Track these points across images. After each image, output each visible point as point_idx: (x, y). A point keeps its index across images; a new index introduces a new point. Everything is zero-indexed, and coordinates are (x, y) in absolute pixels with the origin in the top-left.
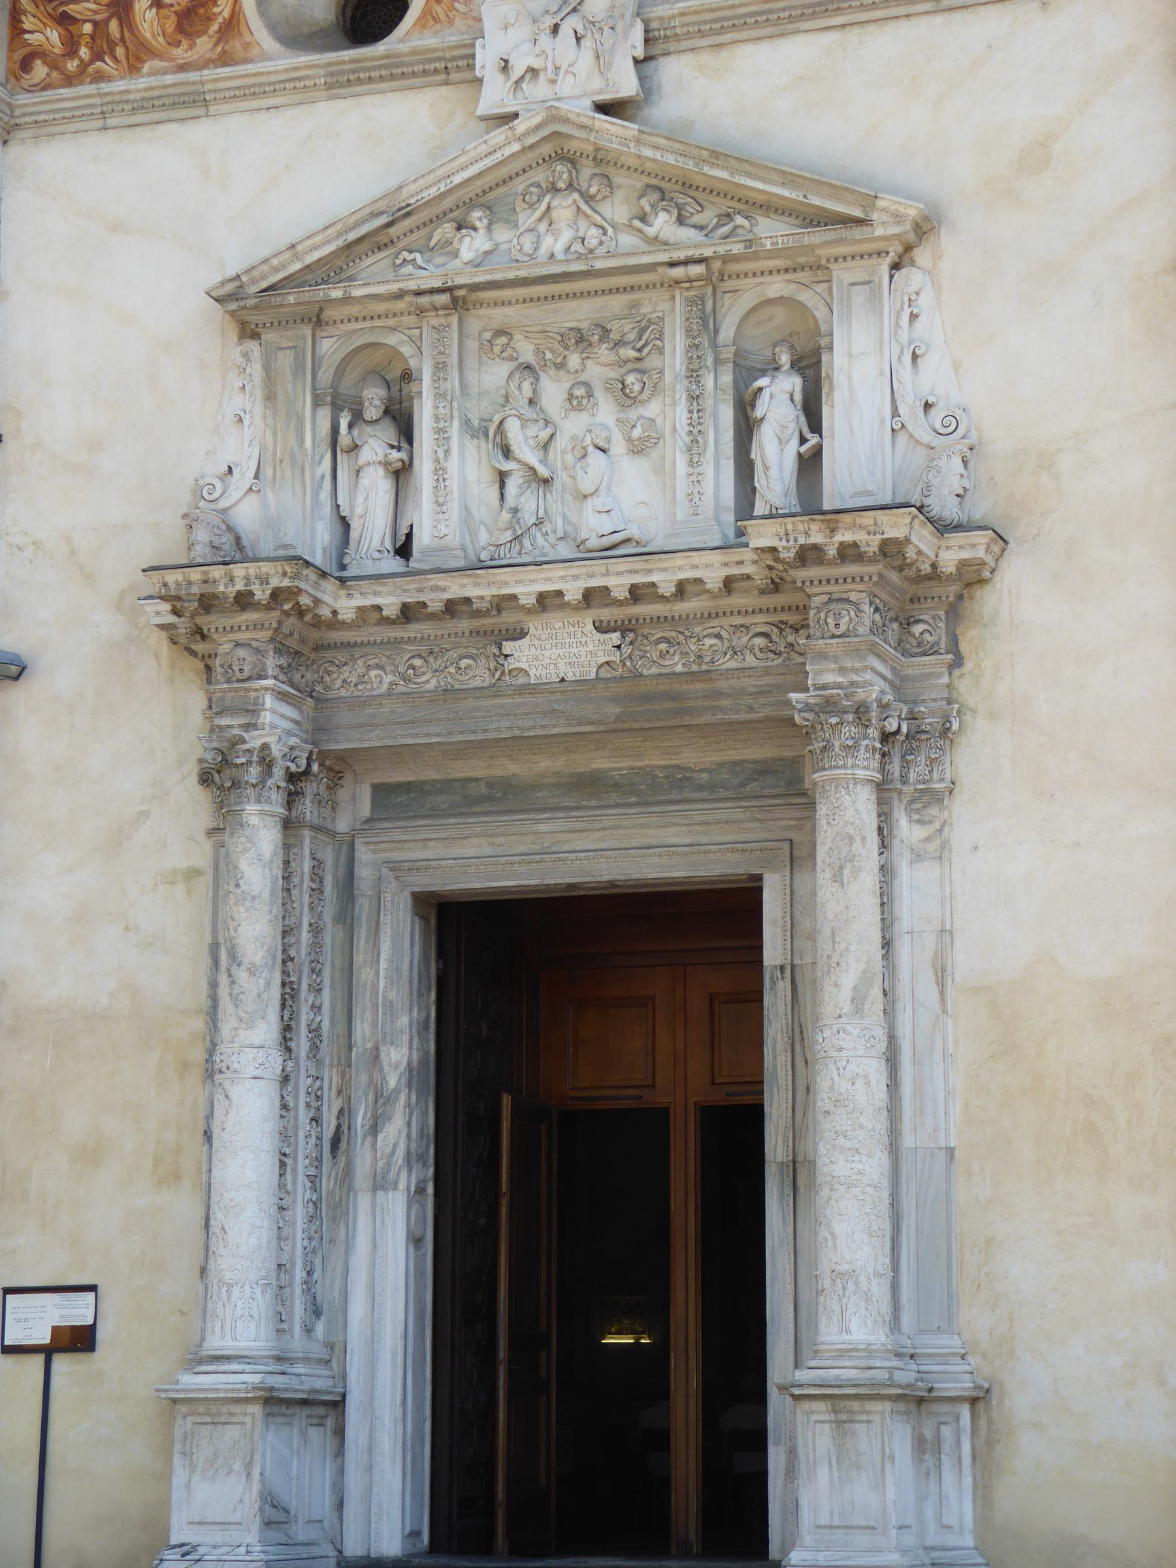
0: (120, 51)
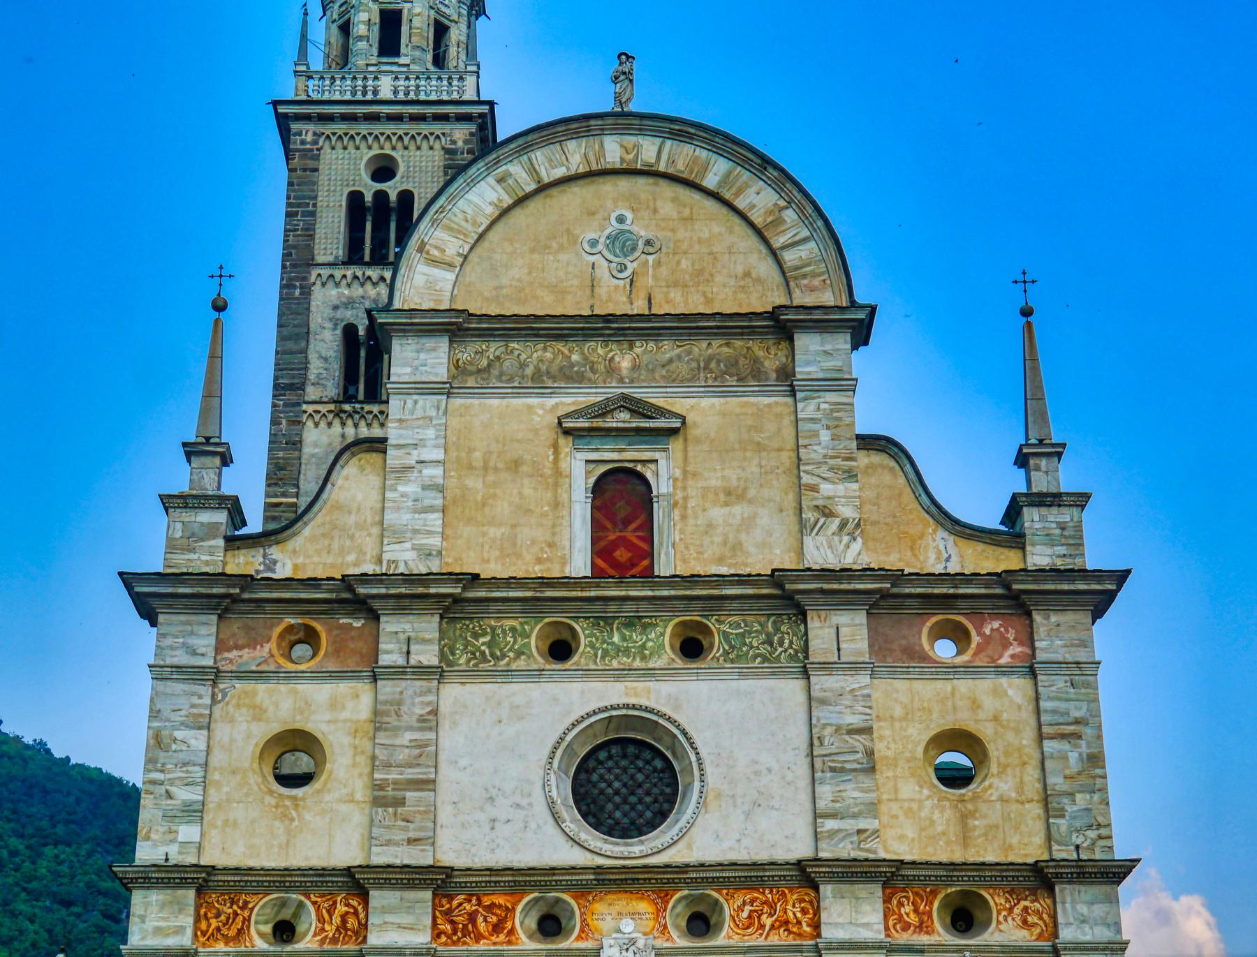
0: (472, 935)
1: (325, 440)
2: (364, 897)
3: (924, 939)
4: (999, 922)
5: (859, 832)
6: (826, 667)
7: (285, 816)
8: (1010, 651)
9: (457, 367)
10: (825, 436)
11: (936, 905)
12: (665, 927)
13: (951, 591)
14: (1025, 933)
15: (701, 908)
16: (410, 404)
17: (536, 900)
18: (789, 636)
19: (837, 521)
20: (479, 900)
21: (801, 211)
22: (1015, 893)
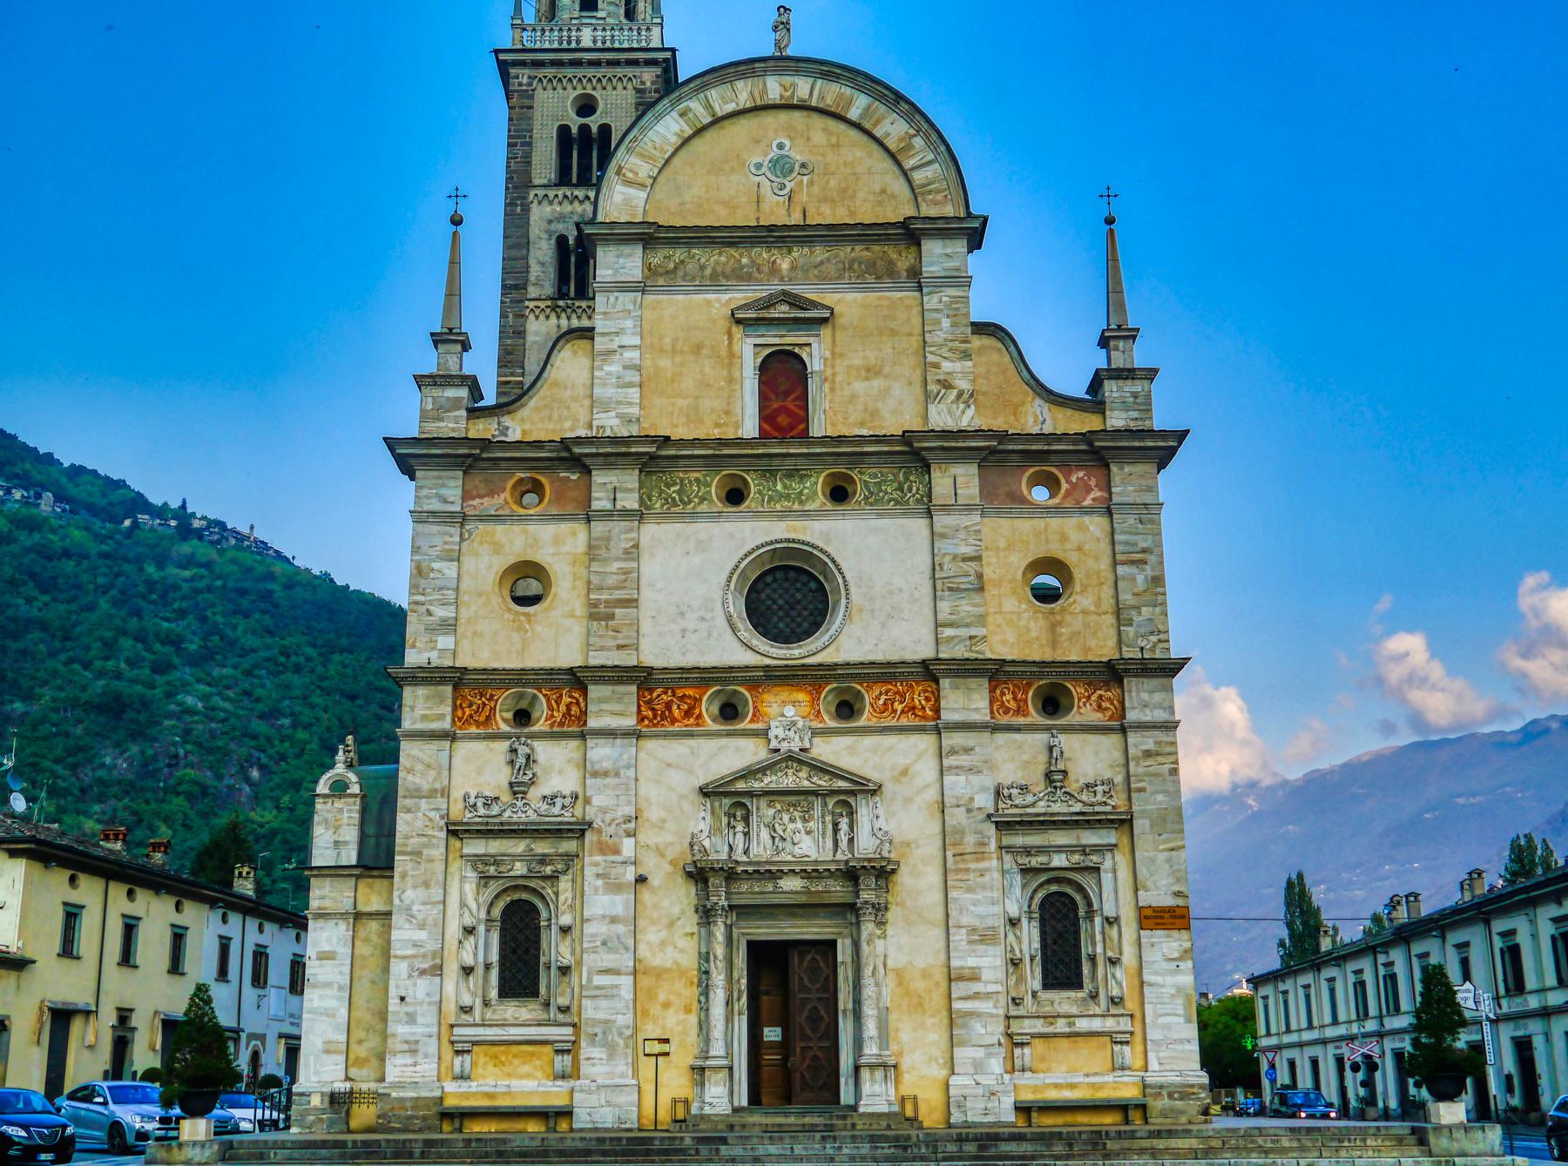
1: (544, 330)
2: (584, 691)
3: (1021, 720)
4: (1079, 707)
5: (971, 638)
6: (945, 508)
7: (521, 629)
8: (1092, 495)
9: (650, 269)
10: (946, 323)
11: (1030, 693)
12: (819, 712)
13: (1046, 448)
14: (1099, 715)
15: (847, 697)
16: (612, 299)
17: (718, 692)
18: (917, 487)
19: (955, 392)
20: (673, 692)
21: (927, 138)
22: (1092, 685)
